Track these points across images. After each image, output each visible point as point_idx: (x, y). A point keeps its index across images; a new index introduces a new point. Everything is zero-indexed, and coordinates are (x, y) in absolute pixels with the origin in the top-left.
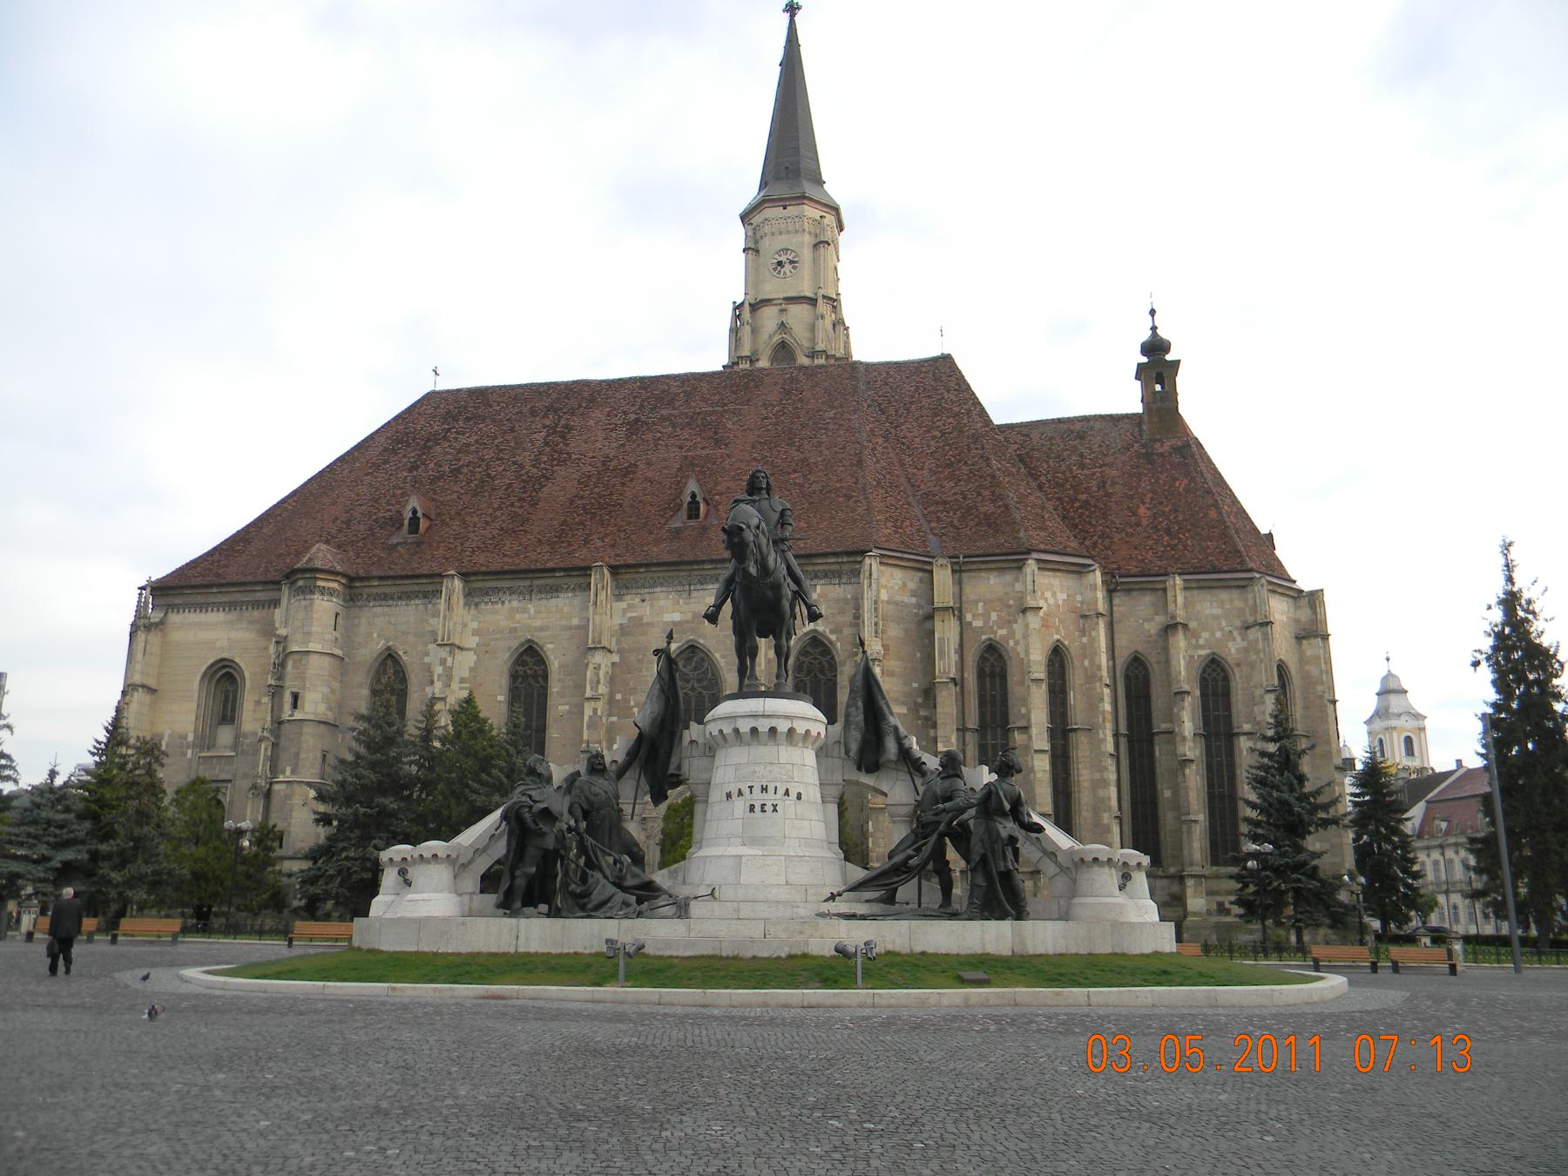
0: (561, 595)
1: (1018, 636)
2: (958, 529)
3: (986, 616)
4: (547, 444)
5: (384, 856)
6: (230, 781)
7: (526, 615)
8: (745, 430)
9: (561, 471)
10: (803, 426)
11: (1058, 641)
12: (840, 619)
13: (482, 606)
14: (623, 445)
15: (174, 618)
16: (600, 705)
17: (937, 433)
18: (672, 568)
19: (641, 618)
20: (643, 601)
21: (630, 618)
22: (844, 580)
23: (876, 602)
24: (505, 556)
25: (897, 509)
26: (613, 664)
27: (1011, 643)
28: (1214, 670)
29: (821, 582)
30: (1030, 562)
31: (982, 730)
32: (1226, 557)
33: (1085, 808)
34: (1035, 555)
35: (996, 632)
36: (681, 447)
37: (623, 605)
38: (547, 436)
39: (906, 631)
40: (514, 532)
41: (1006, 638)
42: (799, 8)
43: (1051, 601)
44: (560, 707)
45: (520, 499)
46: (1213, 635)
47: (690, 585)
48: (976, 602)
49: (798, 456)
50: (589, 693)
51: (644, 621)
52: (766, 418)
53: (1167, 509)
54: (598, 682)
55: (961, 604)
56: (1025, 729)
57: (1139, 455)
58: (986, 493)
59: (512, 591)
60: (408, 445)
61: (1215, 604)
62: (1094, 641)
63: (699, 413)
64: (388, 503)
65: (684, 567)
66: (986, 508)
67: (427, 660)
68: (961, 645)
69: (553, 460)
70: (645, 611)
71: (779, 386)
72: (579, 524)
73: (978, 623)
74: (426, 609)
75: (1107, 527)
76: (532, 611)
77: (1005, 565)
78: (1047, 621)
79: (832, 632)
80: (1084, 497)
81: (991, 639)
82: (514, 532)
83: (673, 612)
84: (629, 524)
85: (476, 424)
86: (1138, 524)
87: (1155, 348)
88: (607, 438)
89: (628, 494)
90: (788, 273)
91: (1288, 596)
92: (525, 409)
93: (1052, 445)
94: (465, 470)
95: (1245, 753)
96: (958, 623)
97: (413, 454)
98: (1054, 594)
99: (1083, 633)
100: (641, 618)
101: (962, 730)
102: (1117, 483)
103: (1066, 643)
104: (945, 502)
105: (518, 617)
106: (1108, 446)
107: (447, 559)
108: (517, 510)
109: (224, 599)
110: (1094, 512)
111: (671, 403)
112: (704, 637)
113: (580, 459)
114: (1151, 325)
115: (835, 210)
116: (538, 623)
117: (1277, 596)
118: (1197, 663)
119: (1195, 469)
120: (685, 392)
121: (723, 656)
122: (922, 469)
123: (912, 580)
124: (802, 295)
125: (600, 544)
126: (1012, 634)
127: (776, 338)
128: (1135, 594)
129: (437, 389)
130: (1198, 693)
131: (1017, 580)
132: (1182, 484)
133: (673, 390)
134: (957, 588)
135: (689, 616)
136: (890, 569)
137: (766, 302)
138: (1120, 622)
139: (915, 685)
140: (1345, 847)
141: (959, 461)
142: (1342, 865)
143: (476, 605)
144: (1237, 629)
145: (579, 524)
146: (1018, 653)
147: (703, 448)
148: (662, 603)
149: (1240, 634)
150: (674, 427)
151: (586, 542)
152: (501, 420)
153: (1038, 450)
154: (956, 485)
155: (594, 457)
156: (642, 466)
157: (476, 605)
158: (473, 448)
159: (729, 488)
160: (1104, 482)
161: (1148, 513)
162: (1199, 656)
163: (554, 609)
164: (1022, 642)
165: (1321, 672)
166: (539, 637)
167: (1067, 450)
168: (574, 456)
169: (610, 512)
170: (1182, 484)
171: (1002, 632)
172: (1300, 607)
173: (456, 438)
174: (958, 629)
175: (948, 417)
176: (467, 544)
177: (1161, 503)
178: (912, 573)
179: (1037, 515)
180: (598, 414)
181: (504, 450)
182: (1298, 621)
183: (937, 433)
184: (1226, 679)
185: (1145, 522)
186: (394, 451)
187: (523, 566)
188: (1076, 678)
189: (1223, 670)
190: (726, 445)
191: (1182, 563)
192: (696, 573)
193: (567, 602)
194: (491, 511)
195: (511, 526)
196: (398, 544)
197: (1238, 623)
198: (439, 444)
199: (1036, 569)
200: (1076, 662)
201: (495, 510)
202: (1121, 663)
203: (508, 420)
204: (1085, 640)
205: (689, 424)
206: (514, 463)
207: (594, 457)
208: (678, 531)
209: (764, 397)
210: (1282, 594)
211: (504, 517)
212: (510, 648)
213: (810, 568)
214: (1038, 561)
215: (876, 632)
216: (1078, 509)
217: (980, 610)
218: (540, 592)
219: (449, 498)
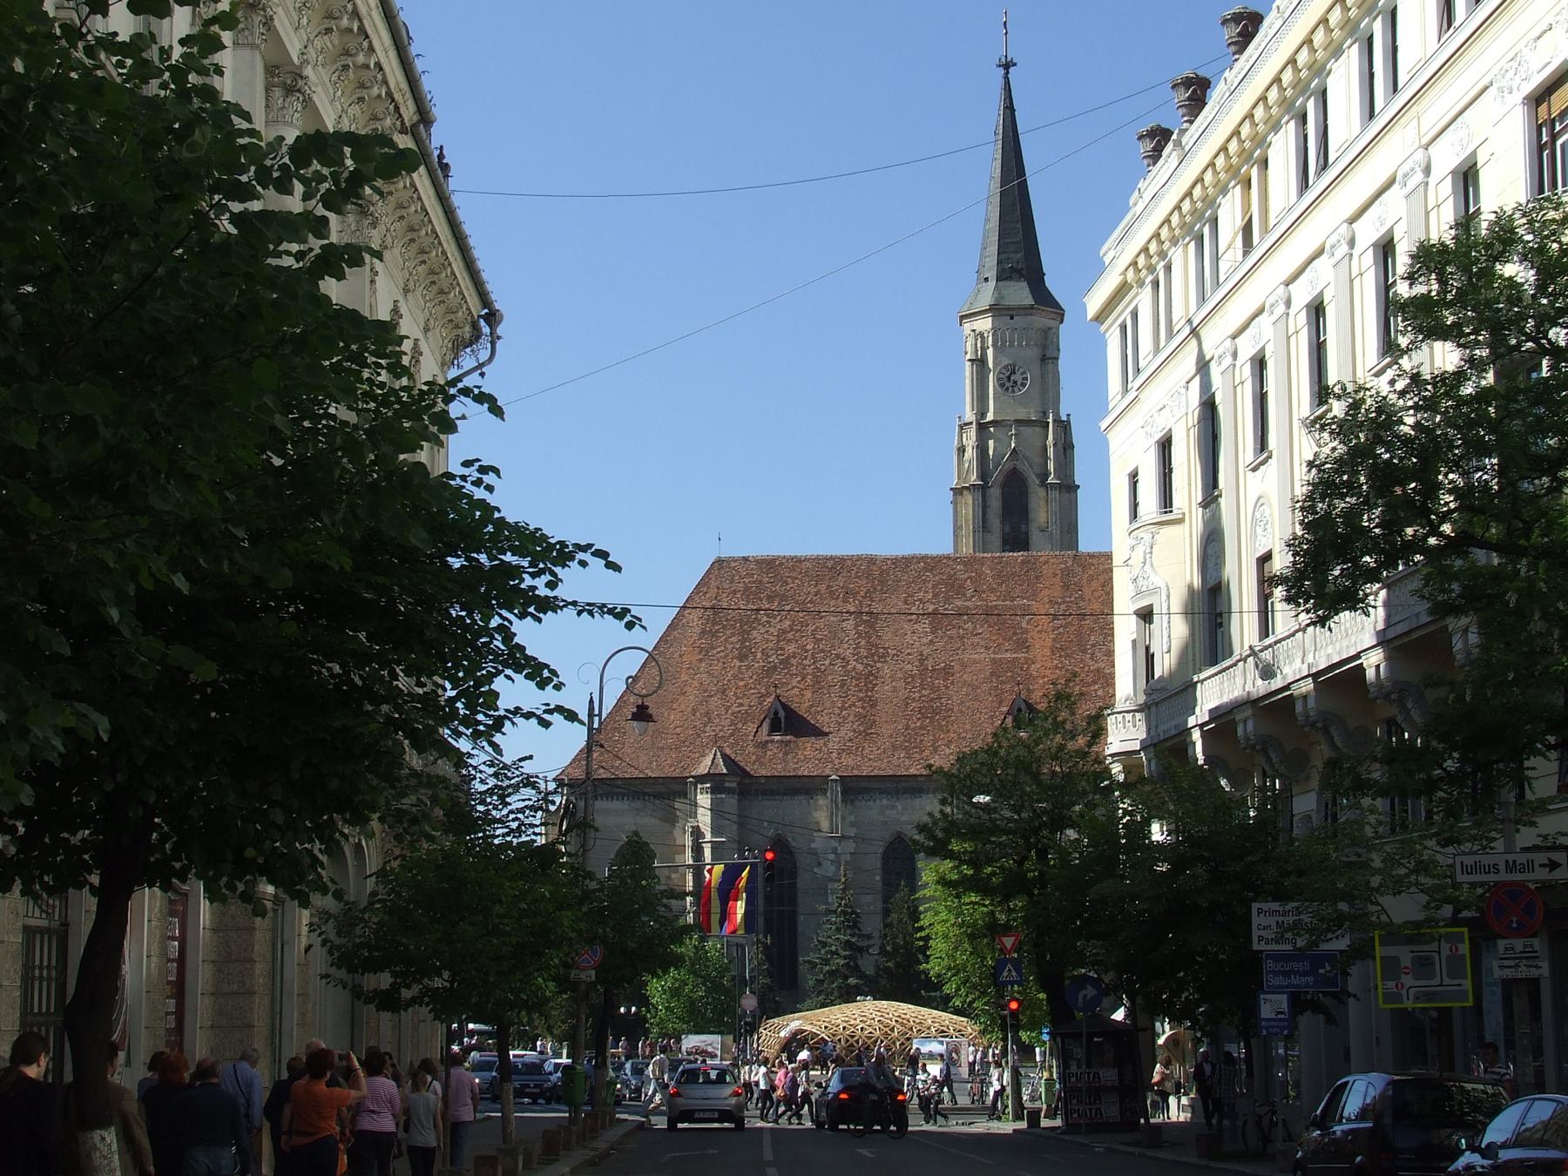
4: (860, 635)
7: (895, 812)
8: (1040, 632)
10: (1092, 630)
13: (857, 803)
14: (931, 641)
24: (870, 760)
36: (987, 648)
38: (857, 625)
40: (868, 734)
42: (1015, 65)
59: (882, 792)
60: (724, 627)
64: (735, 693)
67: (813, 845)
69: (873, 655)
72: (921, 728)
76: (900, 808)
82: (868, 734)
89: (955, 698)
94: (794, 661)
97: (734, 639)
107: (819, 760)
108: (861, 710)
111: (960, 590)
120: (970, 578)
125: (948, 751)
127: (1010, 466)
143: (852, 802)
145: (921, 728)
147: (1007, 651)
151: (936, 750)
155: (909, 654)
156: (957, 668)
157: (852, 802)
158: (790, 636)
169: (945, 718)
173: (768, 622)
176: (830, 745)
180: (896, 603)
181: (822, 639)
186: (713, 634)
195: (862, 729)
196: (767, 742)
203: (810, 602)
206: (838, 656)
207: (909, 654)
209: (1046, 592)
211: (851, 718)
218: (904, 793)
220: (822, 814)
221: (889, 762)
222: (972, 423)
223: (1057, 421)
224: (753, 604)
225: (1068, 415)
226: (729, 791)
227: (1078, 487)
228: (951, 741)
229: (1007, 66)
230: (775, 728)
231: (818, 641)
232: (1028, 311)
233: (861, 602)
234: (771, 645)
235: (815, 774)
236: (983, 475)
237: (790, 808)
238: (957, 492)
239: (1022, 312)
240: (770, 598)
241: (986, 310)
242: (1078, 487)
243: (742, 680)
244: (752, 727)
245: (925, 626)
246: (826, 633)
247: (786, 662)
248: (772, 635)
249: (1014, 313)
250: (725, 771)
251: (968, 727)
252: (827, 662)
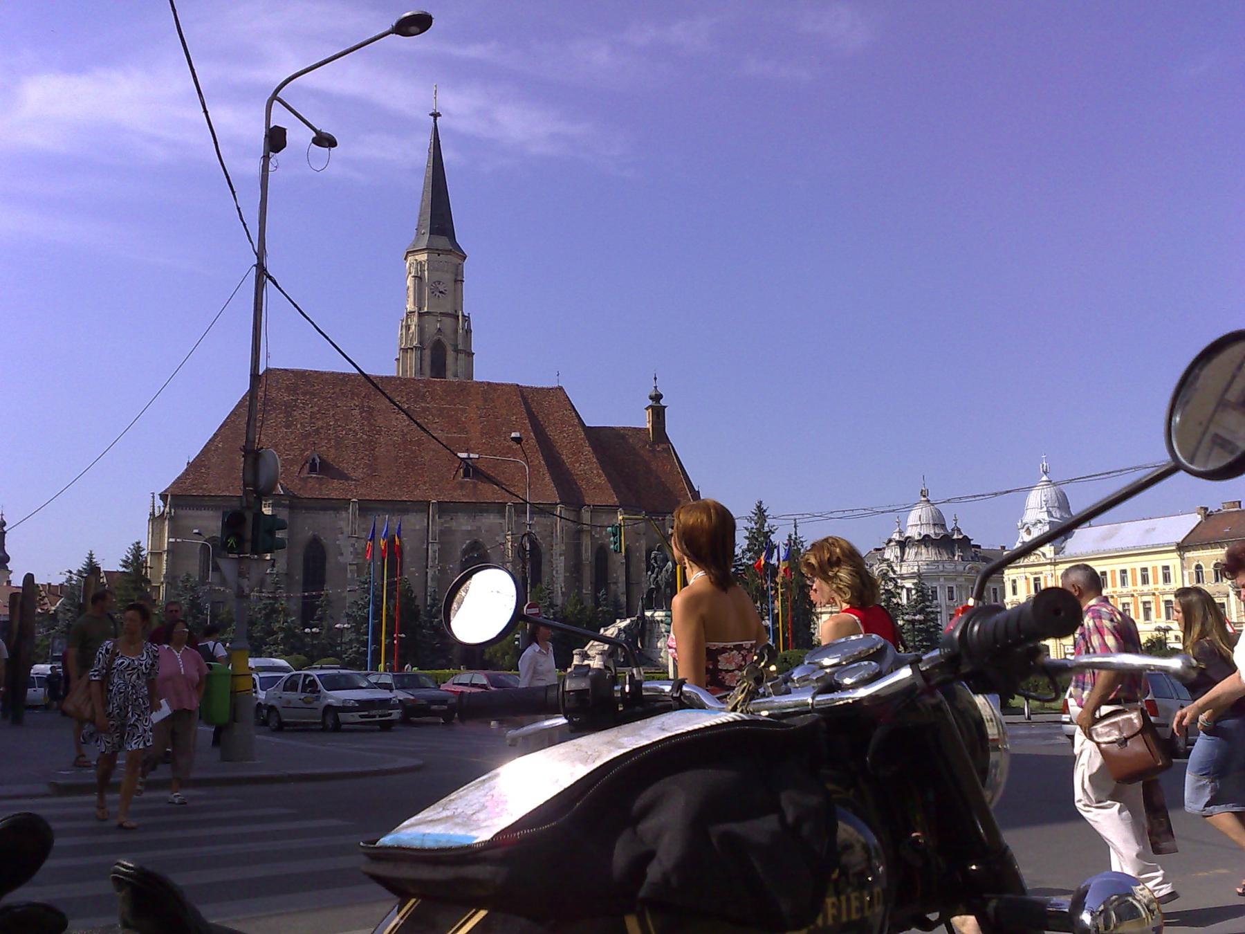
4: (363, 418)
5: (574, 652)
6: (222, 602)
8: (473, 423)
10: (503, 425)
14: (408, 424)
15: (181, 512)
17: (565, 434)
20: (452, 519)
21: (446, 527)
37: (442, 520)
38: (361, 413)
42: (440, 115)
44: (411, 569)
45: (366, 455)
54: (436, 558)
56: (615, 583)
63: (443, 408)
67: (337, 542)
69: (373, 430)
70: (454, 524)
71: (480, 396)
73: (597, 536)
74: (336, 516)
76: (395, 520)
84: (434, 476)
87: (657, 397)
88: (397, 419)
92: (337, 390)
97: (281, 416)
99: (637, 541)
101: (591, 583)
108: (367, 461)
109: (212, 504)
111: (423, 397)
124: (450, 312)
135: (475, 528)
137: (428, 313)
139: (572, 563)
141: (579, 452)
147: (455, 433)
155: (395, 431)
183: (565, 434)
190: (466, 431)
194: (352, 462)
198: (295, 410)
203: (330, 397)
204: (637, 544)
206: (350, 429)
219: (322, 449)
220: (346, 521)
221: (388, 493)
222: (414, 312)
223: (463, 316)
224: (293, 396)
225: (469, 314)
226: (284, 506)
227: (473, 354)
229: (436, 115)
230: (313, 469)
231: (336, 421)
232: (448, 253)
233: (362, 401)
234: (307, 420)
235: (341, 497)
236: (421, 342)
237: (326, 518)
238: (405, 350)
239: (445, 253)
240: (304, 394)
241: (424, 249)
242: (473, 354)
243: (288, 440)
244: (296, 468)
246: (342, 416)
247: (317, 431)
248: (306, 414)
249: (440, 252)
250: (282, 493)
251: (435, 474)
252: (344, 433)
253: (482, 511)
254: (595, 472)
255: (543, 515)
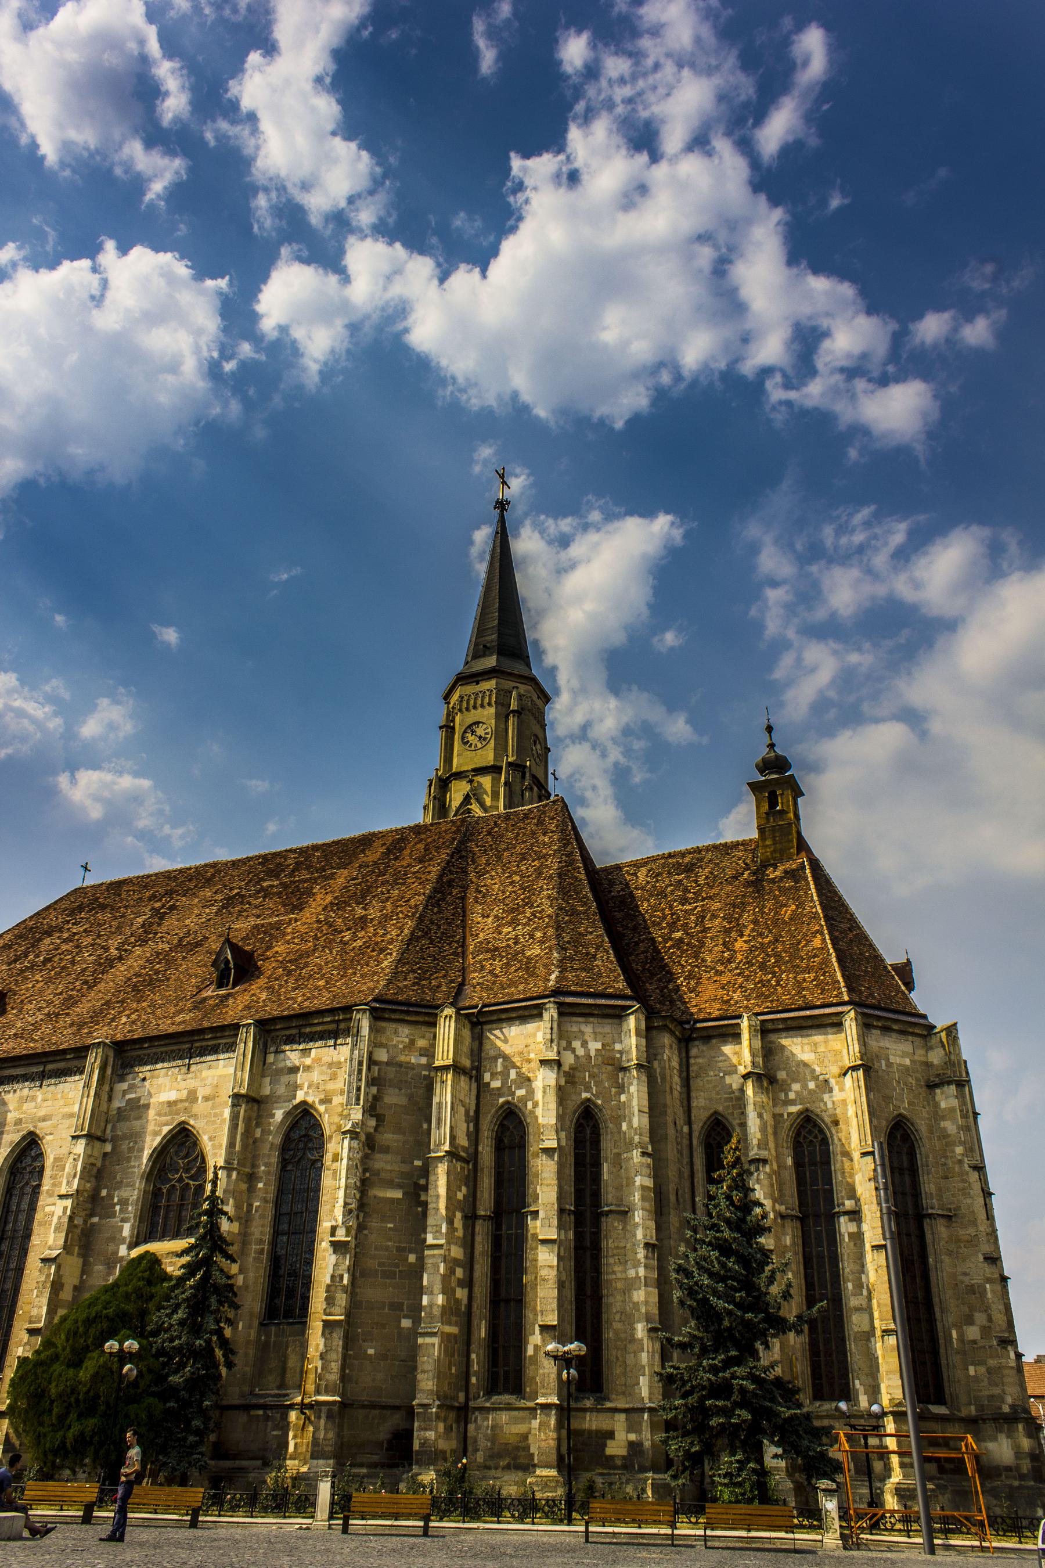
0: (69, 1079)
1: (539, 1096)
2: (496, 976)
3: (505, 1074)
4: (143, 926)
9: (138, 950)
11: (588, 1100)
12: (331, 1086)
14: (209, 920)
16: (68, 1203)
17: (517, 878)
18: (173, 1041)
19: (139, 1098)
22: (339, 1042)
23: (360, 1063)
24: (33, 1040)
25: (435, 959)
26: (105, 1154)
27: (530, 1105)
28: (810, 1132)
29: (319, 1044)
30: (548, 1006)
31: (497, 1217)
32: (823, 990)
33: (617, 1317)
34: (562, 999)
35: (514, 1093)
37: (124, 1086)
39: (411, 1097)
41: (524, 1100)
43: (580, 1052)
45: (86, 982)
46: (805, 1086)
47: (190, 1058)
48: (496, 1059)
49: (360, 912)
50: (63, 1191)
51: (142, 1102)
52: (353, 879)
53: (767, 940)
54: (75, 1176)
55: (480, 1060)
57: (748, 884)
58: (538, 935)
59: (26, 1078)
61: (806, 1047)
62: (630, 1095)
65: (185, 1039)
66: (528, 953)
68: (477, 1111)
72: (122, 1002)
73: (496, 1084)
75: (697, 966)
76: (39, 1099)
77: (526, 1013)
78: (574, 1076)
79: (322, 1102)
80: (678, 935)
81: (508, 1102)
83: (171, 1090)
85: (97, 913)
86: (729, 961)
89: (182, 969)
90: (479, 745)
91: (913, 1034)
93: (657, 881)
94: (56, 959)
95: (847, 1240)
96: (474, 1085)
98: (585, 1044)
99: (622, 1088)
100: (139, 1098)
101: (471, 1218)
102: (714, 916)
103: (599, 1102)
104: (496, 949)
105: (25, 1106)
106: (715, 876)
108: (74, 993)
110: (687, 950)
112: (195, 1117)
113: (161, 938)
114: (769, 742)
115: (533, 680)
116: (42, 1113)
117: (894, 1035)
118: (787, 1124)
119: (806, 893)
121: (211, 1139)
122: (488, 917)
123: (423, 1037)
126: (531, 1092)
128: (714, 1041)
129: (85, 885)
130: (789, 1161)
131: (538, 1029)
132: (787, 913)
133: (289, 862)
134: (477, 1042)
136: (394, 1025)
138: (697, 1077)
140: (1006, 1372)
141: (526, 904)
142: (1003, 1401)
144: (834, 1077)
145: (118, 1002)
146: (537, 1118)
148: (160, 1080)
149: (837, 1083)
150: (265, 897)
151: (113, 1020)
152: (120, 907)
153: (642, 889)
154: (514, 929)
158: (76, 937)
159: (277, 952)
160: (704, 917)
161: (745, 946)
162: (789, 1114)
163: (59, 1096)
164: (540, 1104)
165: (960, 1128)
166: (42, 1128)
167: (671, 885)
168: (159, 935)
170: (787, 913)
171: (521, 1093)
172: (931, 1048)
174: (474, 1092)
175: (534, 861)
177: (760, 935)
178: (424, 1028)
179: (587, 954)
182: (928, 1065)
184: (825, 1142)
185: (739, 957)
187: (39, 1050)
188: (608, 1147)
189: (821, 1131)
191: (771, 1001)
192: (198, 1044)
193: (73, 1085)
197: (835, 1070)
199: (555, 1016)
200: (611, 1125)
201: (56, 994)
202: (697, 1127)
204: (623, 1098)
205: (281, 893)
208: (205, 999)
210: (901, 1032)
212: (12, 1142)
213: (308, 1030)
214: (555, 1002)
215: (358, 1099)
216: (670, 948)
217: (499, 1069)
228: (137, 1011)
245: (215, 909)
253: (204, 1052)
254: (538, 935)
255: (332, 1042)
